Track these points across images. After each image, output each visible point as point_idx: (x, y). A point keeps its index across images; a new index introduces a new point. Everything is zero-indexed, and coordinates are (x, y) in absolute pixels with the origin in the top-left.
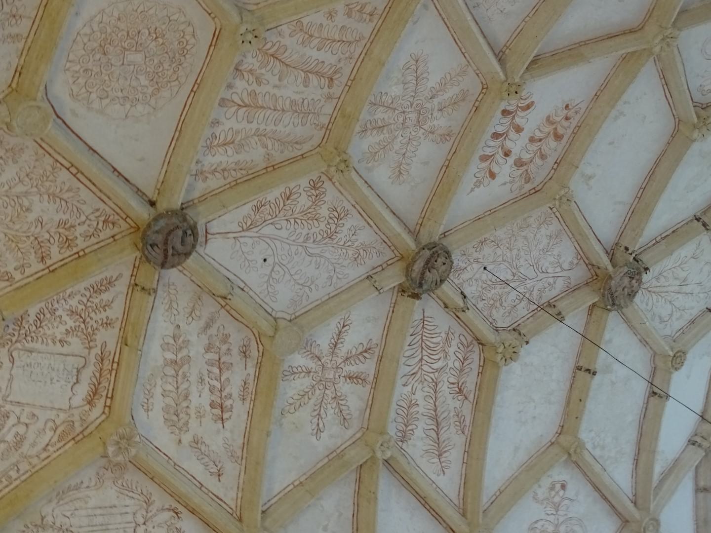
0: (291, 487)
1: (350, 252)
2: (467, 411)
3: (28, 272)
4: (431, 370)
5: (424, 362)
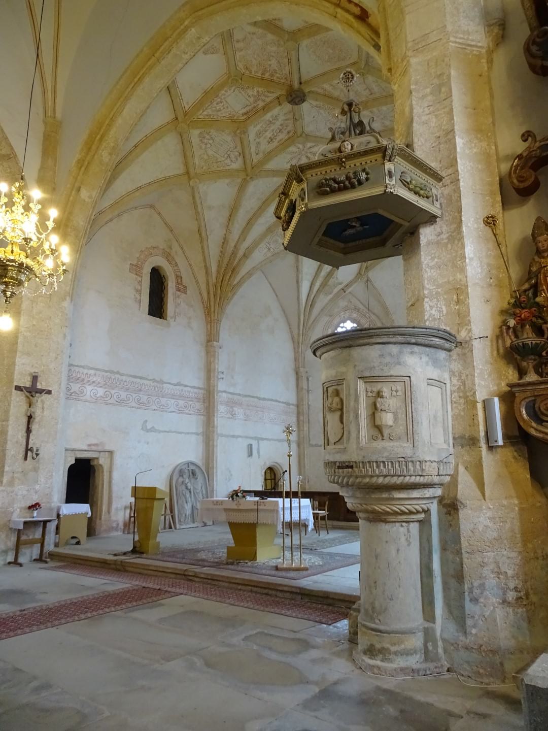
3: (257, 74)
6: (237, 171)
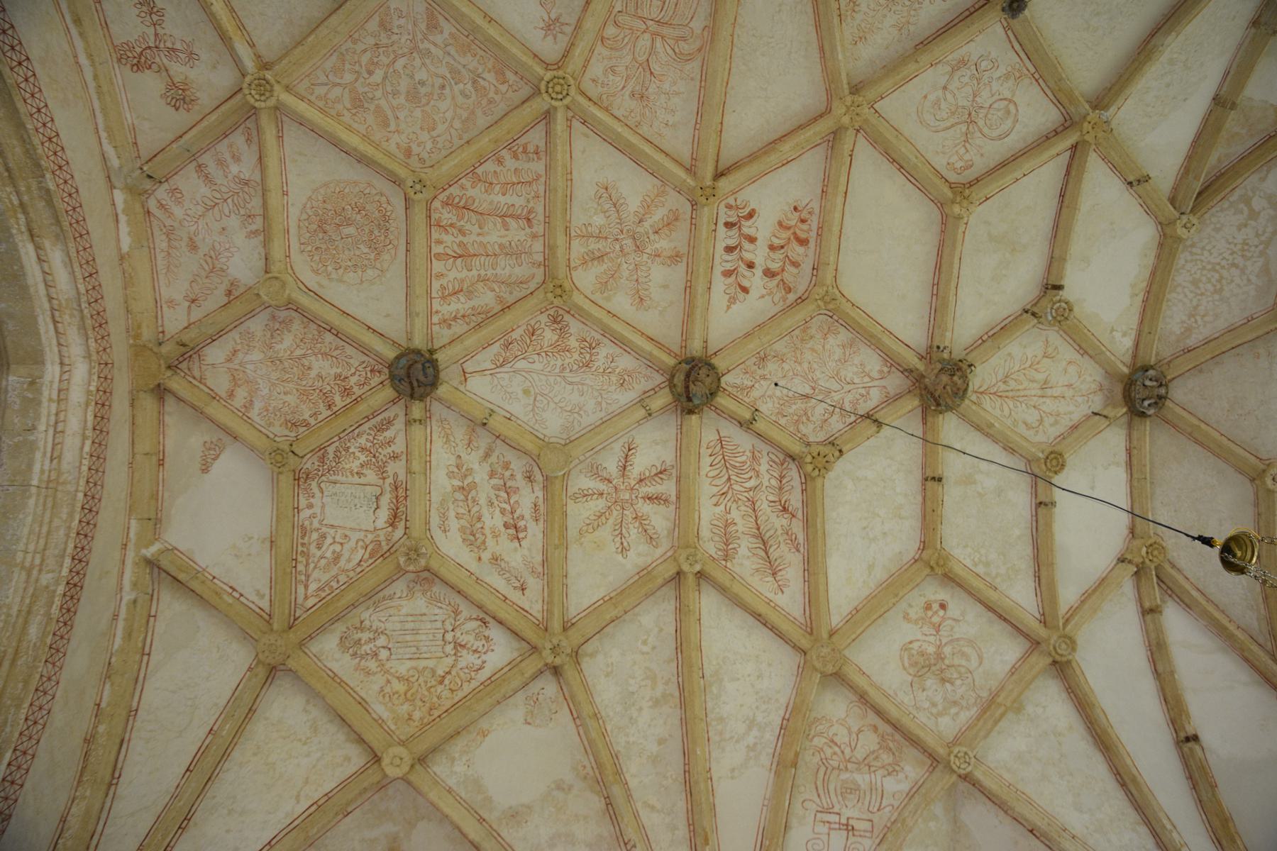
0: (601, 602)
1: (614, 379)
2: (797, 528)
3: (320, 418)
4: (744, 490)
5: (732, 482)
6: (513, 665)
